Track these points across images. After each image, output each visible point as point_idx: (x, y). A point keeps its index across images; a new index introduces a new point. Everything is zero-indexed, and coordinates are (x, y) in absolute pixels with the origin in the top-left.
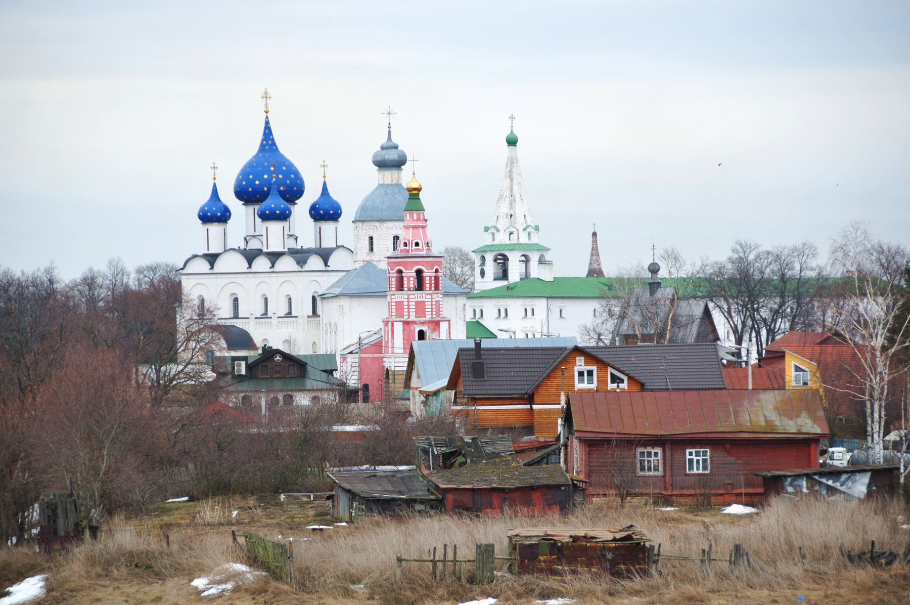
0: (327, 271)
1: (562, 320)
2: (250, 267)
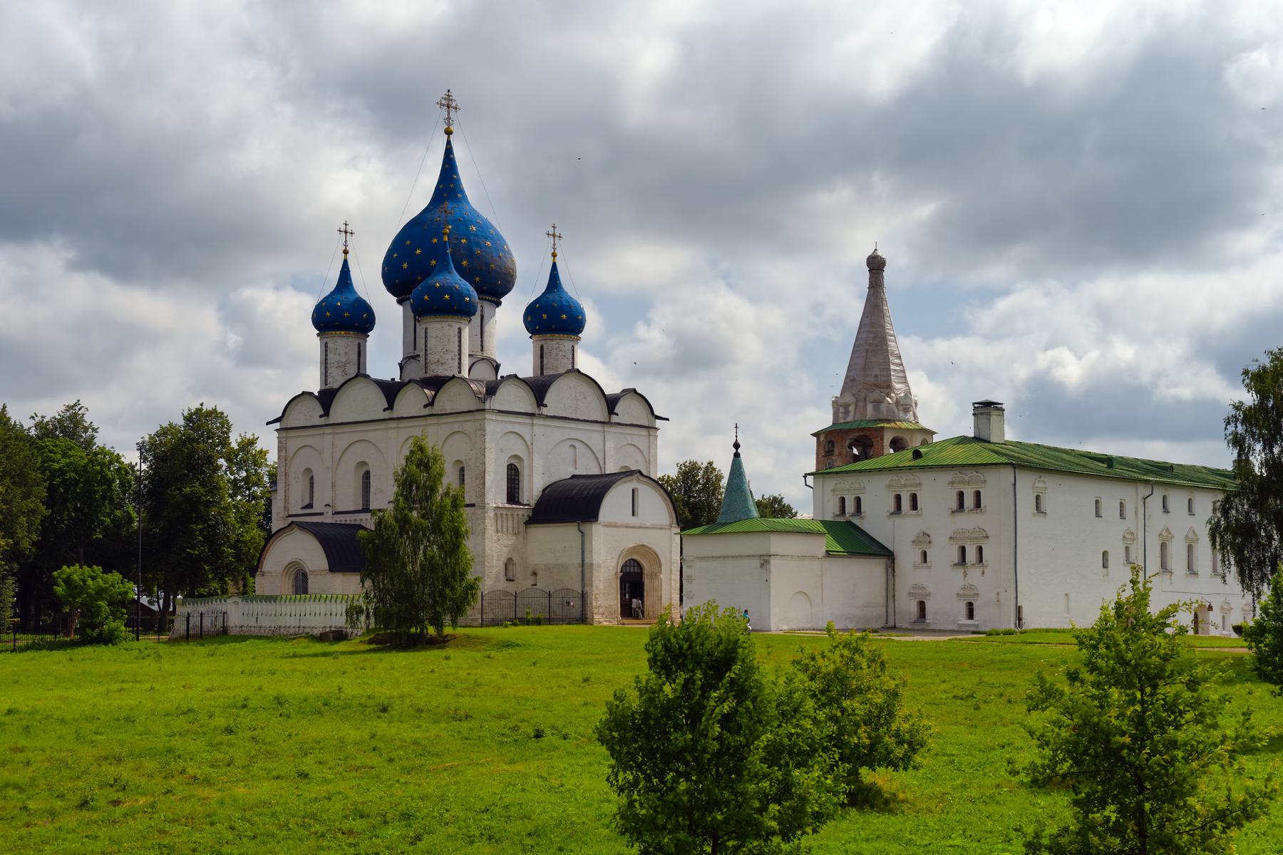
0: (541, 416)
1: (1040, 519)
2: (391, 406)
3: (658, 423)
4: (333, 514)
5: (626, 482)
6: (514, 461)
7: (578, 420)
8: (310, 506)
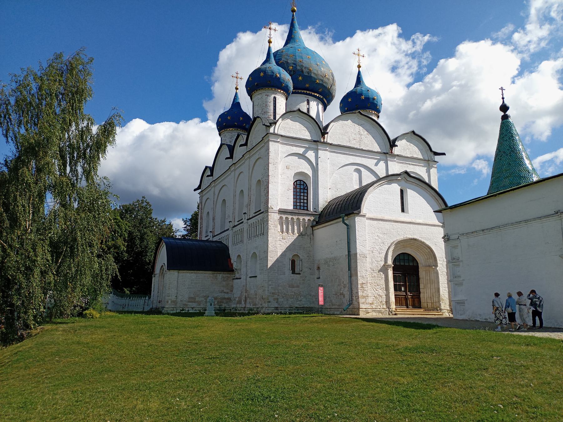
3: (437, 158)
4: (213, 237)
7: (362, 150)
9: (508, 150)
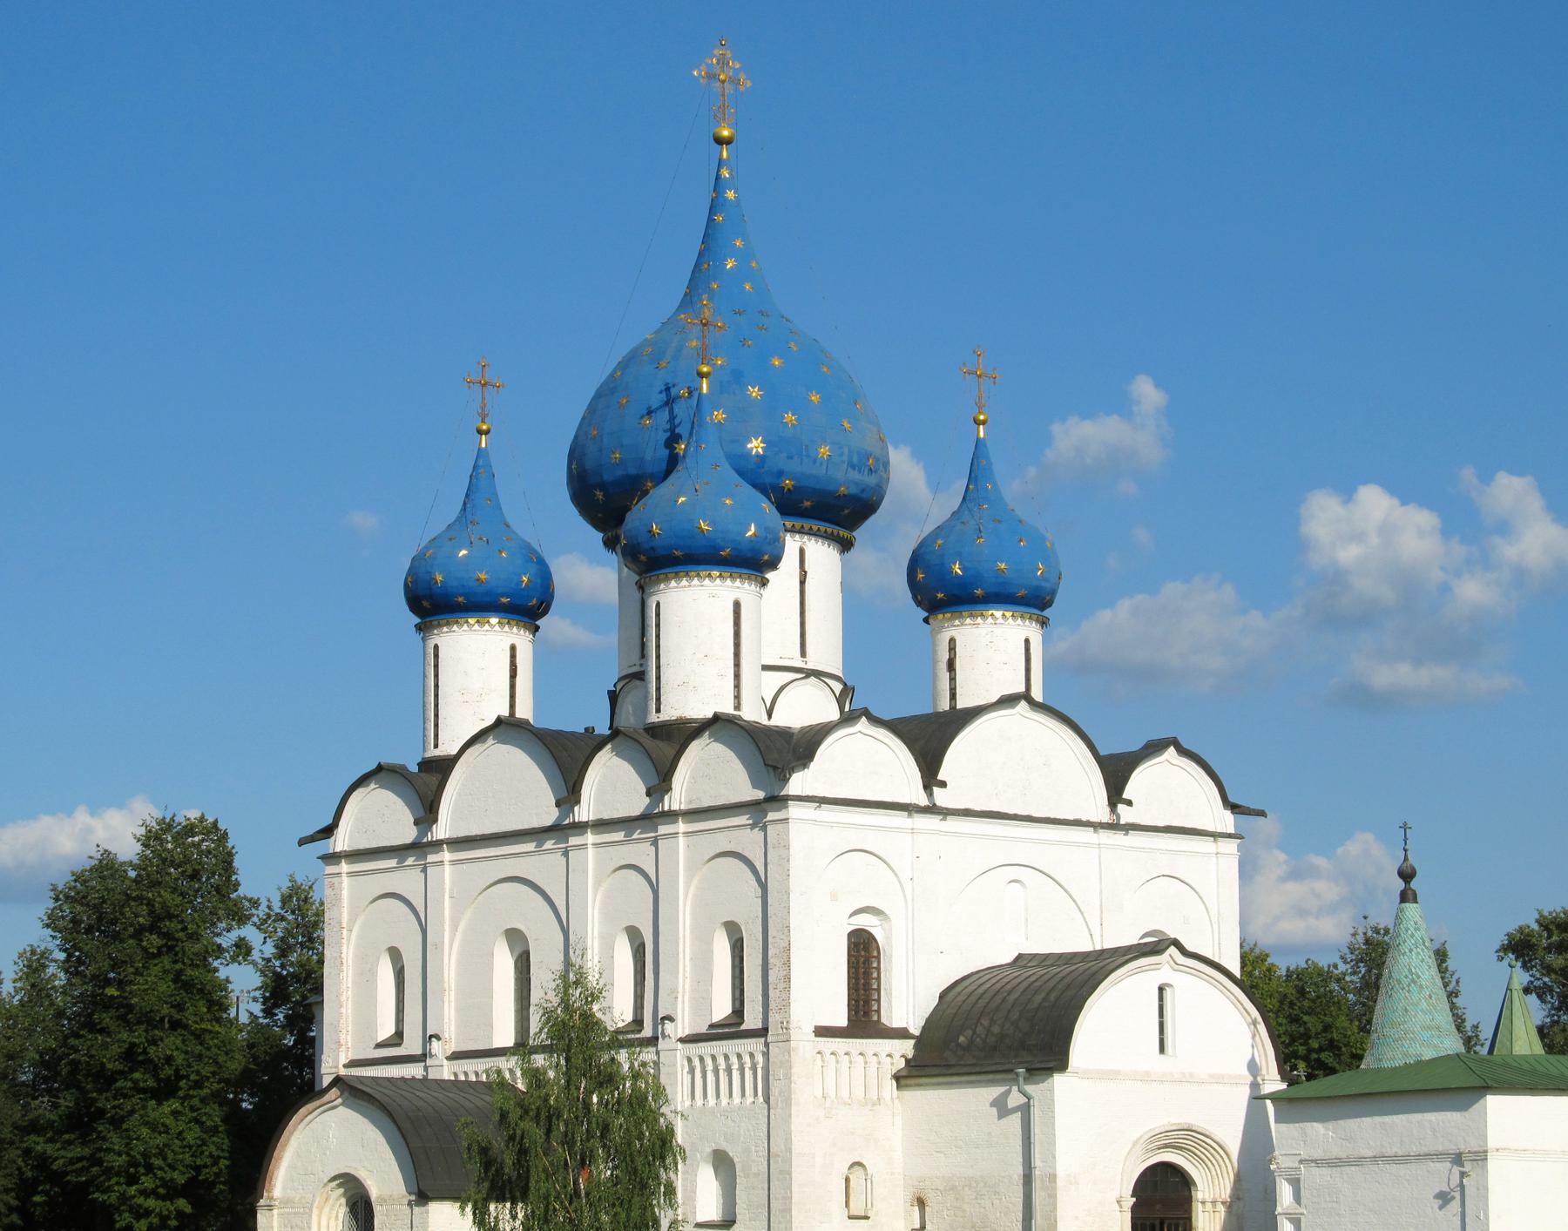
5: (1141, 970)
6: (865, 921)
8: (399, 1036)
9: (1406, 977)
